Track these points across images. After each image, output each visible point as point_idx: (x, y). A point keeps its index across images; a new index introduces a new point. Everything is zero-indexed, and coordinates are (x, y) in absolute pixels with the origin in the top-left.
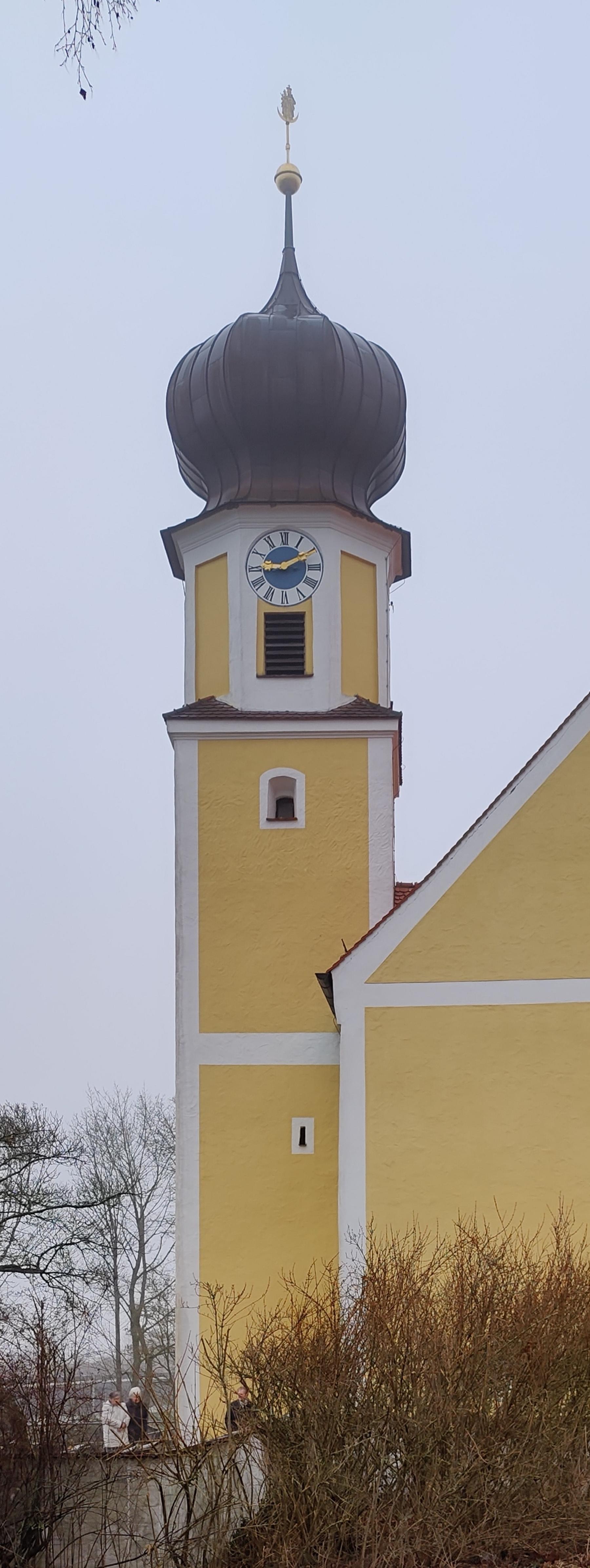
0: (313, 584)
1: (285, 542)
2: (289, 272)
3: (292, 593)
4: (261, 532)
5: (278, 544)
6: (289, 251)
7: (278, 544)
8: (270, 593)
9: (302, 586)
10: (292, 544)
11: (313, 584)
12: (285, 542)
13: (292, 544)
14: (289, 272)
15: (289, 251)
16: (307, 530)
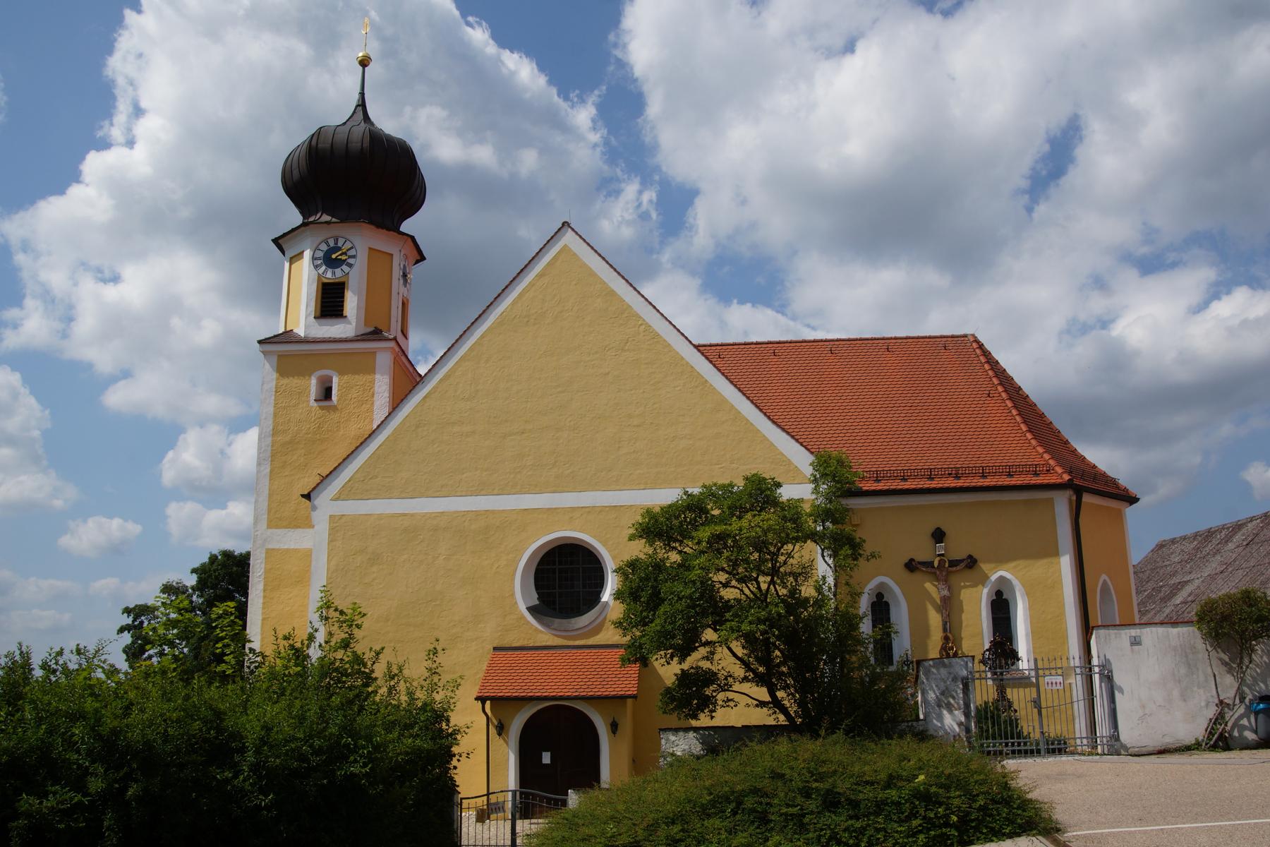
0: (350, 266)
1: (336, 243)
2: (362, 104)
3: (338, 272)
4: (320, 239)
5: (332, 244)
6: (362, 94)
7: (332, 244)
8: (325, 271)
9: (344, 267)
10: (340, 244)
11: (350, 266)
12: (336, 243)
13: (340, 244)
14: (362, 104)
15: (362, 94)
16: (351, 238)
